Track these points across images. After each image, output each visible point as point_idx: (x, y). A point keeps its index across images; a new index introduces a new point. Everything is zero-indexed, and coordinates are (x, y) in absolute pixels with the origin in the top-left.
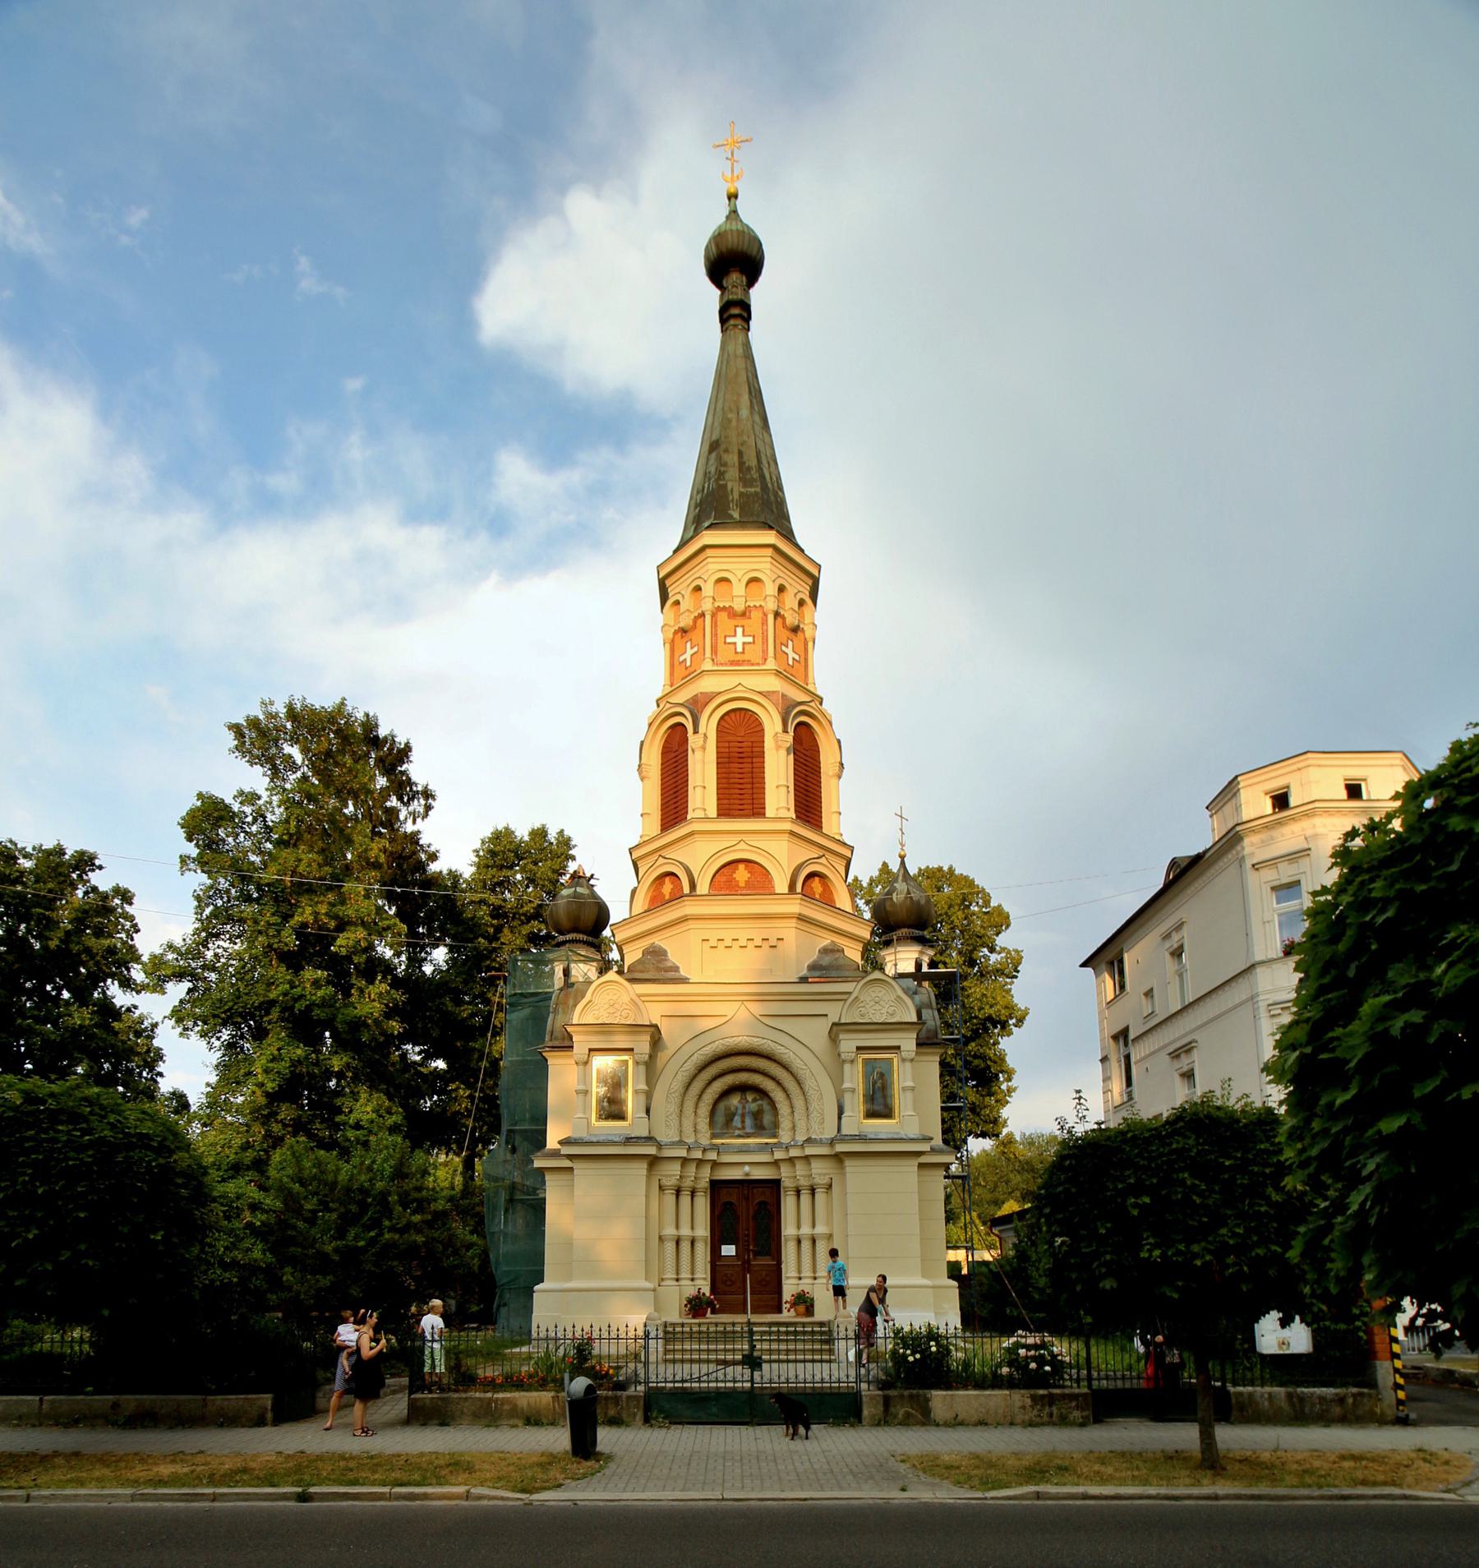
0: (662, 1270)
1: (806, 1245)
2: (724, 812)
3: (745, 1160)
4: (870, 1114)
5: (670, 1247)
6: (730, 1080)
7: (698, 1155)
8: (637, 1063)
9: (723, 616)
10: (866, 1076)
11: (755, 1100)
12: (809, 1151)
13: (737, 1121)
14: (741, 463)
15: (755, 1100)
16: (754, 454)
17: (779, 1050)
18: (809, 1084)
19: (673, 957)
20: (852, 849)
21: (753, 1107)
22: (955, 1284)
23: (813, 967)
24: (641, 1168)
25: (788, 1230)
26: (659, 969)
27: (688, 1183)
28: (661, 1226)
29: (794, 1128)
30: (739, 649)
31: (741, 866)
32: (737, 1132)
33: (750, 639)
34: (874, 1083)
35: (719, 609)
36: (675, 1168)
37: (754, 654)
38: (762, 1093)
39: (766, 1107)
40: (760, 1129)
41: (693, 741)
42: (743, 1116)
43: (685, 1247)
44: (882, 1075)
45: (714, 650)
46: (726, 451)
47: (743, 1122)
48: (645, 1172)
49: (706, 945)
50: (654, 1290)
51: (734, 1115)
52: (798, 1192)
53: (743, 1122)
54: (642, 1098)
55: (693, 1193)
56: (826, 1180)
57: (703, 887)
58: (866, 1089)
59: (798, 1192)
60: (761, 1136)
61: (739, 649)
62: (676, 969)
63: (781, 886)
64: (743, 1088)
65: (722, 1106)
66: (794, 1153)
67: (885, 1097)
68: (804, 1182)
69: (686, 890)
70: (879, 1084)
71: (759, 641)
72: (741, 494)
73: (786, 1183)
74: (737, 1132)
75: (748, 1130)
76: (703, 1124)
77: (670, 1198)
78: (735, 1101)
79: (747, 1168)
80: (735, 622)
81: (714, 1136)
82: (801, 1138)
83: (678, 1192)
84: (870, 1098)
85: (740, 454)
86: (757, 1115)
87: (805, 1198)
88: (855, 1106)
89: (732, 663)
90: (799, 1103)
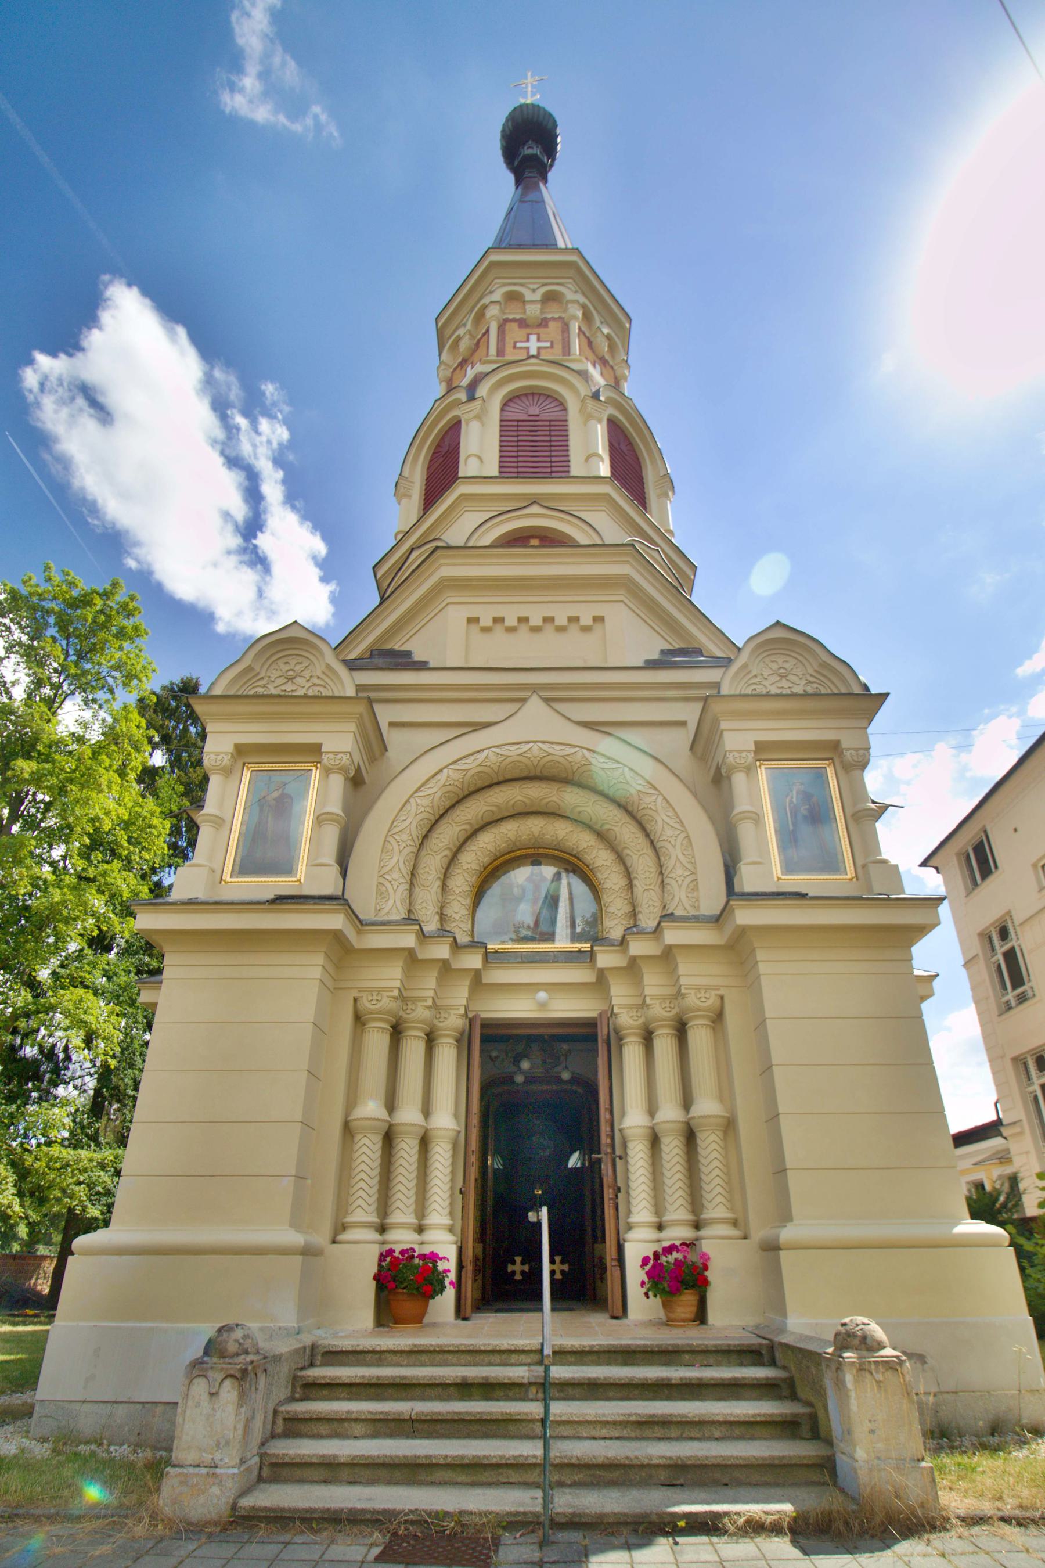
0: (342, 1205)
5: (368, 1150)
6: (511, 831)
7: (441, 951)
8: (327, 771)
9: (515, 326)
12: (672, 936)
20: (694, 568)
24: (311, 967)
25: (633, 1119)
27: (420, 1013)
28: (352, 1100)
33: (548, 344)
36: (391, 975)
38: (573, 864)
43: (407, 1151)
48: (317, 972)
49: (474, 629)
50: (308, 1252)
54: (331, 835)
55: (431, 1040)
56: (712, 1001)
59: (648, 1038)
65: (495, 890)
66: (638, 947)
71: (558, 347)
73: (627, 1019)
77: (377, 1042)
78: (521, 876)
79: (542, 995)
80: (528, 331)
82: (648, 922)
83: (397, 1032)
87: (665, 1046)
90: (643, 864)
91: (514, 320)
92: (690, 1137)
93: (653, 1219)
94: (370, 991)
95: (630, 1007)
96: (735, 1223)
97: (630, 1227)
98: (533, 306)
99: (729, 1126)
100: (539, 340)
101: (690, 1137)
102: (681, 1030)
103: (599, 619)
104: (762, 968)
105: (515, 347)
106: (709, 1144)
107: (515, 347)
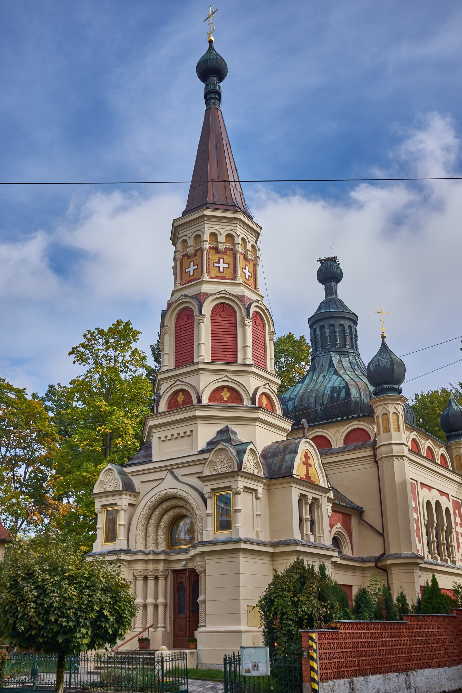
30: (221, 270)
31: (225, 390)
37: (229, 273)
41: (197, 319)
45: (208, 271)
57: (205, 401)
61: (221, 270)
69: (195, 401)
80: (219, 256)
89: (217, 277)
91: (212, 248)
98: (222, 245)
100: (224, 263)
105: (214, 266)
107: (214, 266)
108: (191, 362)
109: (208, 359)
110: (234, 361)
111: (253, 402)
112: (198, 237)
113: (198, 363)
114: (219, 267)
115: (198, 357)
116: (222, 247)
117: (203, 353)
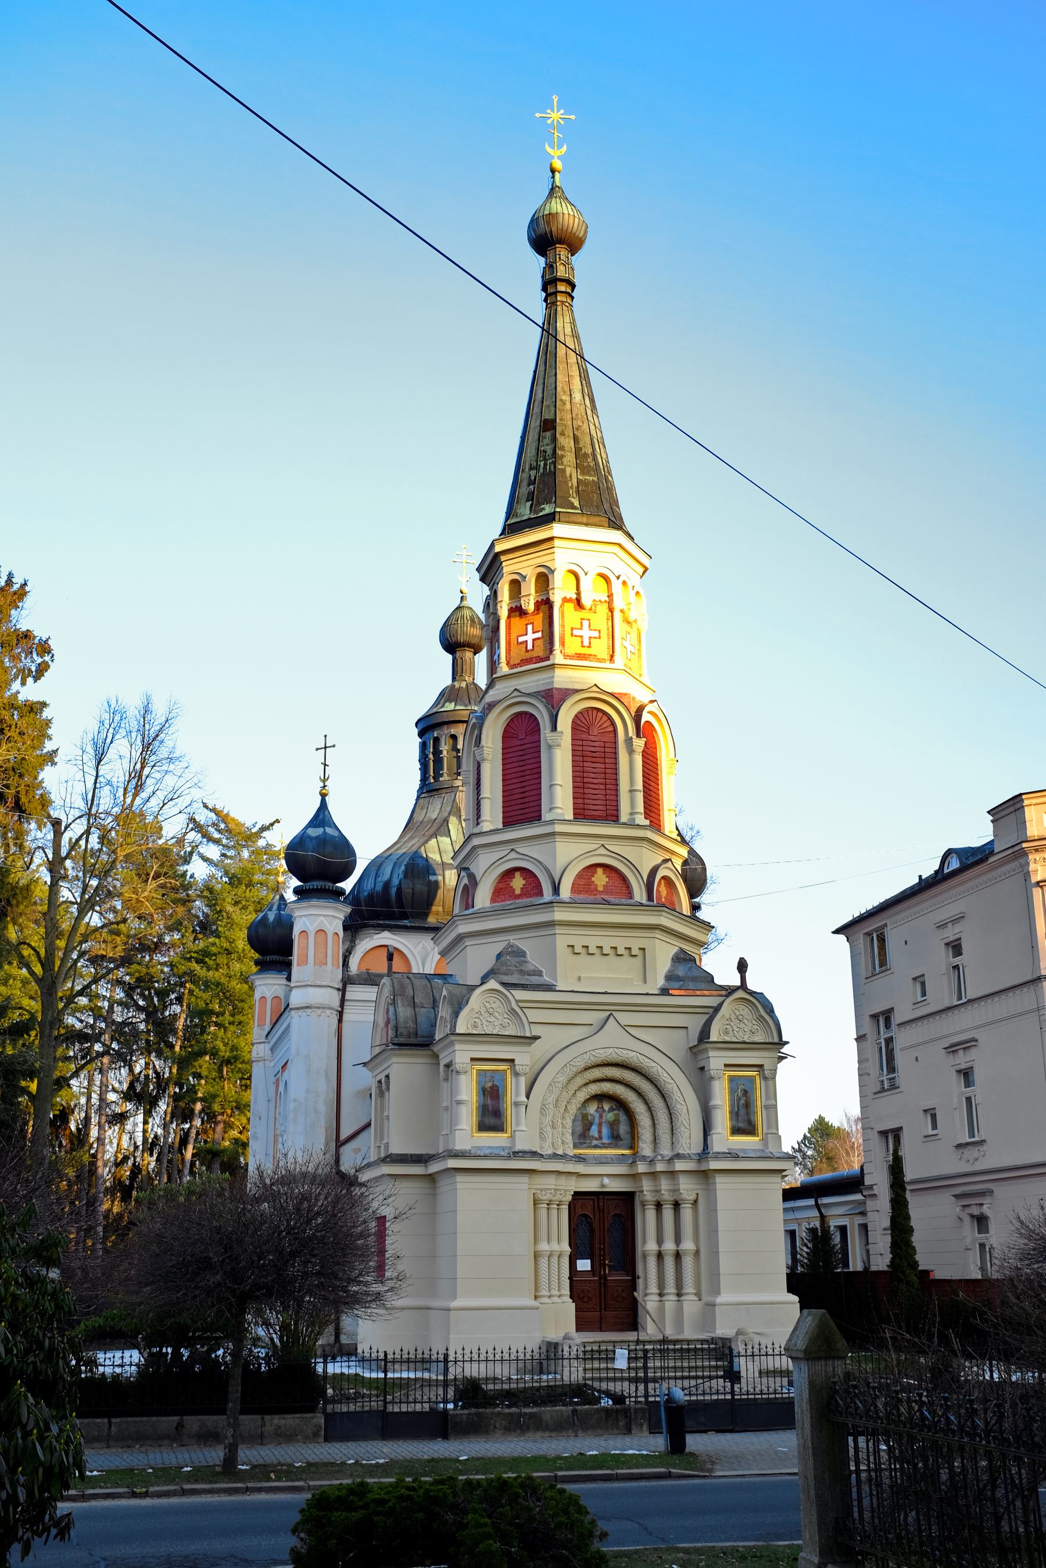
1: (669, 1263)
2: (581, 814)
3: (604, 1174)
4: (736, 1131)
9: (570, 607)
10: (732, 1092)
11: (611, 1110)
13: (594, 1131)
14: (578, 451)
15: (611, 1110)
16: (588, 441)
17: (646, 1063)
18: (676, 1097)
19: (533, 961)
21: (610, 1116)
22: (796, 1299)
23: (670, 977)
25: (652, 1246)
26: (522, 972)
29: (655, 1140)
30: (586, 644)
31: (600, 870)
32: (595, 1142)
34: (739, 1100)
35: (565, 600)
39: (623, 1118)
40: (616, 1139)
42: (600, 1125)
44: (745, 1092)
46: (563, 434)
47: (600, 1132)
51: (591, 1124)
52: (659, 1206)
53: (600, 1132)
56: (693, 1197)
57: (565, 892)
58: (732, 1106)
59: (659, 1206)
60: (616, 1147)
62: (539, 973)
63: (639, 894)
64: (620, 1104)
66: (660, 1167)
67: (748, 1113)
68: (667, 1196)
70: (742, 1102)
72: (579, 481)
73: (649, 1196)
74: (595, 1142)
75: (605, 1141)
76: (569, 1138)
78: (592, 1109)
81: (575, 1146)
82: (666, 1151)
84: (735, 1114)
85: (576, 439)
86: (613, 1125)
87: (668, 1213)
88: (722, 1120)
89: (580, 656)
91: (570, 600)
92: (678, 1256)
93: (657, 1291)
94: (541, 1190)
95: (652, 1191)
96: (696, 1294)
97: (646, 1295)
99: (697, 1253)
101: (678, 1256)
102: (676, 1205)
103: (644, 949)
104: (718, 1186)
106: (688, 1262)
108: (538, 818)
109: (571, 817)
110: (612, 816)
111: (650, 898)
112: (544, 580)
113: (552, 822)
114: (581, 637)
115: (551, 809)
116: (586, 601)
117: (559, 803)
